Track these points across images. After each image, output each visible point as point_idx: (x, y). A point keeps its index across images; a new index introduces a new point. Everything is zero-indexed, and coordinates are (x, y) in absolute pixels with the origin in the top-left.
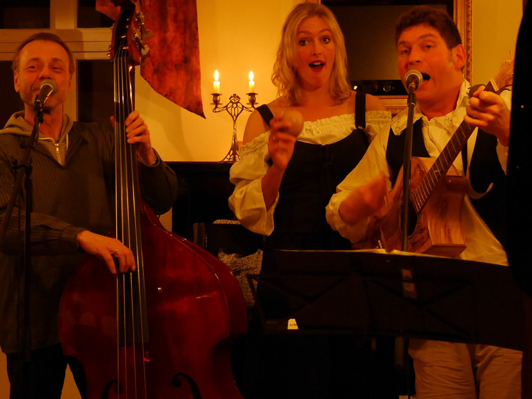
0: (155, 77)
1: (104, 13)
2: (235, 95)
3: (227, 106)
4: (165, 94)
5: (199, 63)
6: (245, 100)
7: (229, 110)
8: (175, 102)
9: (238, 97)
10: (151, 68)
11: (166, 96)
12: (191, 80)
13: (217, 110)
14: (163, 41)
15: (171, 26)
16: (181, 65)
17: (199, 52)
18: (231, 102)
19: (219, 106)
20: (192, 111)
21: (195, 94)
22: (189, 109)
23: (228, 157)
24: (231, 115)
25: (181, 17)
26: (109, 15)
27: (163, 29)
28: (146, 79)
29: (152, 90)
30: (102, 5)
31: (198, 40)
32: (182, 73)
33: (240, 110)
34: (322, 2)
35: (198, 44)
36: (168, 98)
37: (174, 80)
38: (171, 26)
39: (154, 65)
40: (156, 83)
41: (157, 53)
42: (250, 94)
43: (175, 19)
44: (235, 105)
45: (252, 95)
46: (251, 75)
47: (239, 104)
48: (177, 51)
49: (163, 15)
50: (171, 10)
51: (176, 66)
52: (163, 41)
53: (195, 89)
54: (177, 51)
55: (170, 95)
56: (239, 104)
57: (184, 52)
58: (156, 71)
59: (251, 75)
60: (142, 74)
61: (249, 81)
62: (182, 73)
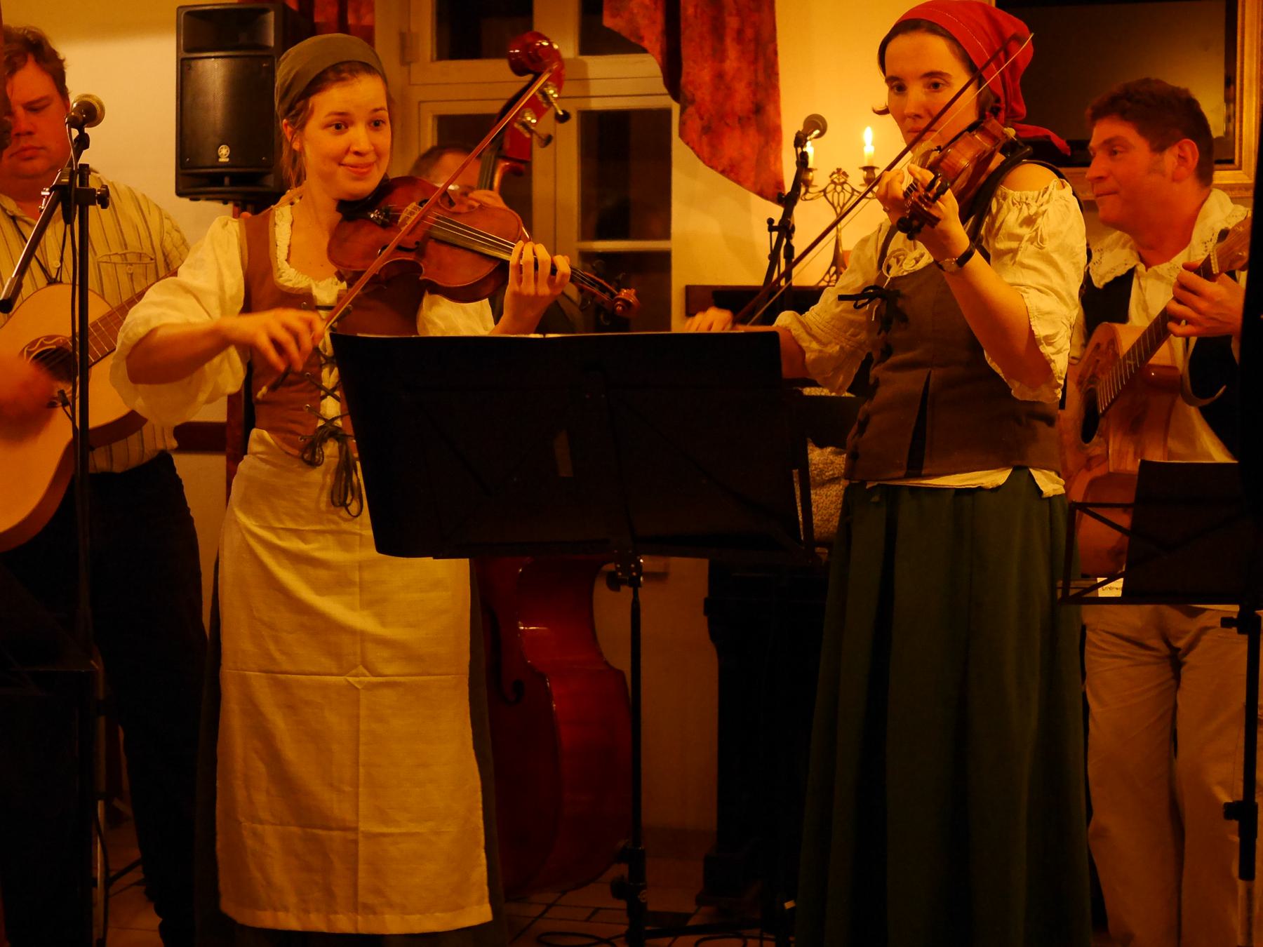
0: (705, 139)
1: (616, 30)
2: (839, 170)
3: (824, 191)
4: (720, 168)
5: (778, 114)
6: (857, 180)
7: (829, 196)
8: (738, 182)
9: (844, 174)
10: (698, 124)
11: (723, 172)
12: (767, 143)
13: (808, 196)
14: (719, 76)
15: (732, 52)
16: (749, 118)
17: (779, 95)
18: (833, 182)
19: (811, 190)
20: (766, 198)
21: (773, 168)
22: (761, 194)
23: (827, 278)
24: (832, 204)
25: (749, 33)
26: (625, 33)
27: (719, 55)
28: (687, 144)
29: (701, 163)
30: (613, 16)
31: (777, 74)
32: (752, 131)
33: (848, 195)
34: (998, 5)
35: (777, 80)
36: (728, 177)
37: (735, 145)
38: (732, 52)
39: (702, 119)
40: (706, 150)
41: (707, 98)
42: (865, 169)
43: (740, 36)
44: (839, 188)
45: (870, 169)
46: (868, 135)
47: (846, 186)
48: (742, 95)
49: (718, 31)
50: (733, 23)
51: (740, 119)
52: (719, 76)
53: (772, 159)
54: (742, 95)
55: (731, 171)
56: (846, 186)
57: (755, 94)
58: (707, 130)
59: (868, 135)
60: (681, 135)
61: (862, 145)
62: (752, 131)
